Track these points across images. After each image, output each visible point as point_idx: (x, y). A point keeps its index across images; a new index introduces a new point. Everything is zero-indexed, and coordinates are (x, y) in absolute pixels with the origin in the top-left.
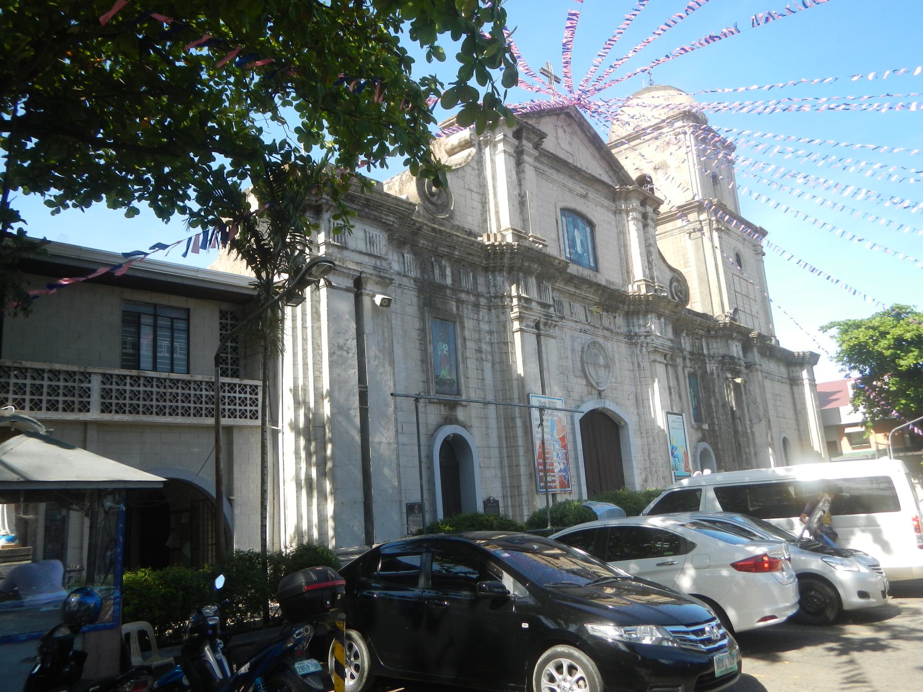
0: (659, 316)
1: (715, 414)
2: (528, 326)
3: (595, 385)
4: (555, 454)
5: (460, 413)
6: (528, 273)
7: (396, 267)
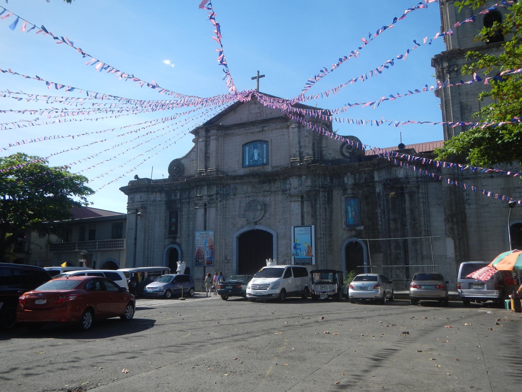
0: (300, 176)
1: (379, 219)
2: (200, 206)
3: (251, 220)
4: (206, 252)
5: (178, 240)
6: (202, 186)
7: (159, 199)
